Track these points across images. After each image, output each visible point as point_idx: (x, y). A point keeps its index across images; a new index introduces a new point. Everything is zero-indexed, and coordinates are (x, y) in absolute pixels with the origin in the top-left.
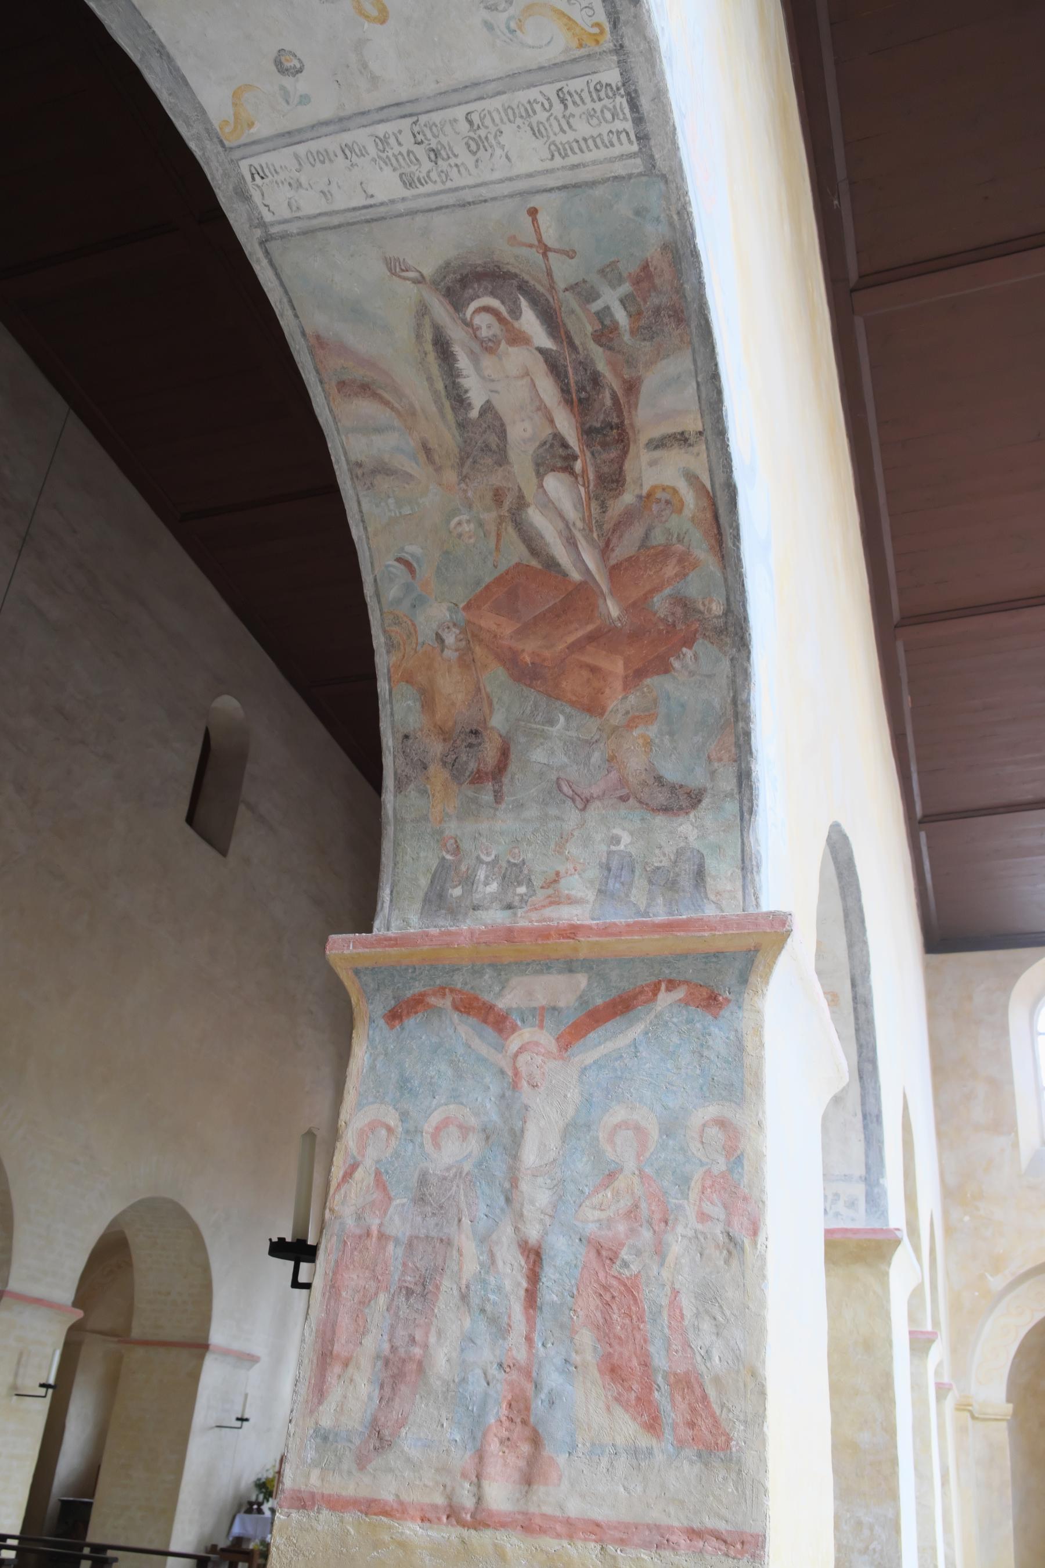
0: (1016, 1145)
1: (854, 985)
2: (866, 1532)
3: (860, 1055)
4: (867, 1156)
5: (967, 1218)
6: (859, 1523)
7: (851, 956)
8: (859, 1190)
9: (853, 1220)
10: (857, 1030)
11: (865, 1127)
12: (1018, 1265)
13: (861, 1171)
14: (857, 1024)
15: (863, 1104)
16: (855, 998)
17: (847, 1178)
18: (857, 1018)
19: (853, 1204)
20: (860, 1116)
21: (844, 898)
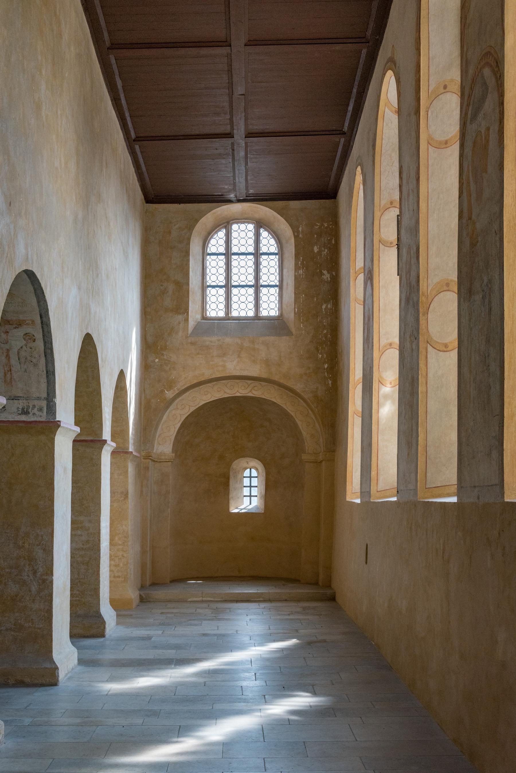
0: (187, 320)
1: (41, 317)
2: (40, 538)
3: (45, 346)
4: (48, 389)
5: (157, 360)
6: (38, 535)
7: (39, 306)
8: (44, 404)
9: (41, 416)
10: (44, 336)
11: (47, 376)
13: (45, 395)
14: (43, 333)
15: (46, 367)
16: (42, 323)
17: (39, 398)
18: (43, 331)
19: (41, 409)
20: (45, 372)
21: (33, 285)
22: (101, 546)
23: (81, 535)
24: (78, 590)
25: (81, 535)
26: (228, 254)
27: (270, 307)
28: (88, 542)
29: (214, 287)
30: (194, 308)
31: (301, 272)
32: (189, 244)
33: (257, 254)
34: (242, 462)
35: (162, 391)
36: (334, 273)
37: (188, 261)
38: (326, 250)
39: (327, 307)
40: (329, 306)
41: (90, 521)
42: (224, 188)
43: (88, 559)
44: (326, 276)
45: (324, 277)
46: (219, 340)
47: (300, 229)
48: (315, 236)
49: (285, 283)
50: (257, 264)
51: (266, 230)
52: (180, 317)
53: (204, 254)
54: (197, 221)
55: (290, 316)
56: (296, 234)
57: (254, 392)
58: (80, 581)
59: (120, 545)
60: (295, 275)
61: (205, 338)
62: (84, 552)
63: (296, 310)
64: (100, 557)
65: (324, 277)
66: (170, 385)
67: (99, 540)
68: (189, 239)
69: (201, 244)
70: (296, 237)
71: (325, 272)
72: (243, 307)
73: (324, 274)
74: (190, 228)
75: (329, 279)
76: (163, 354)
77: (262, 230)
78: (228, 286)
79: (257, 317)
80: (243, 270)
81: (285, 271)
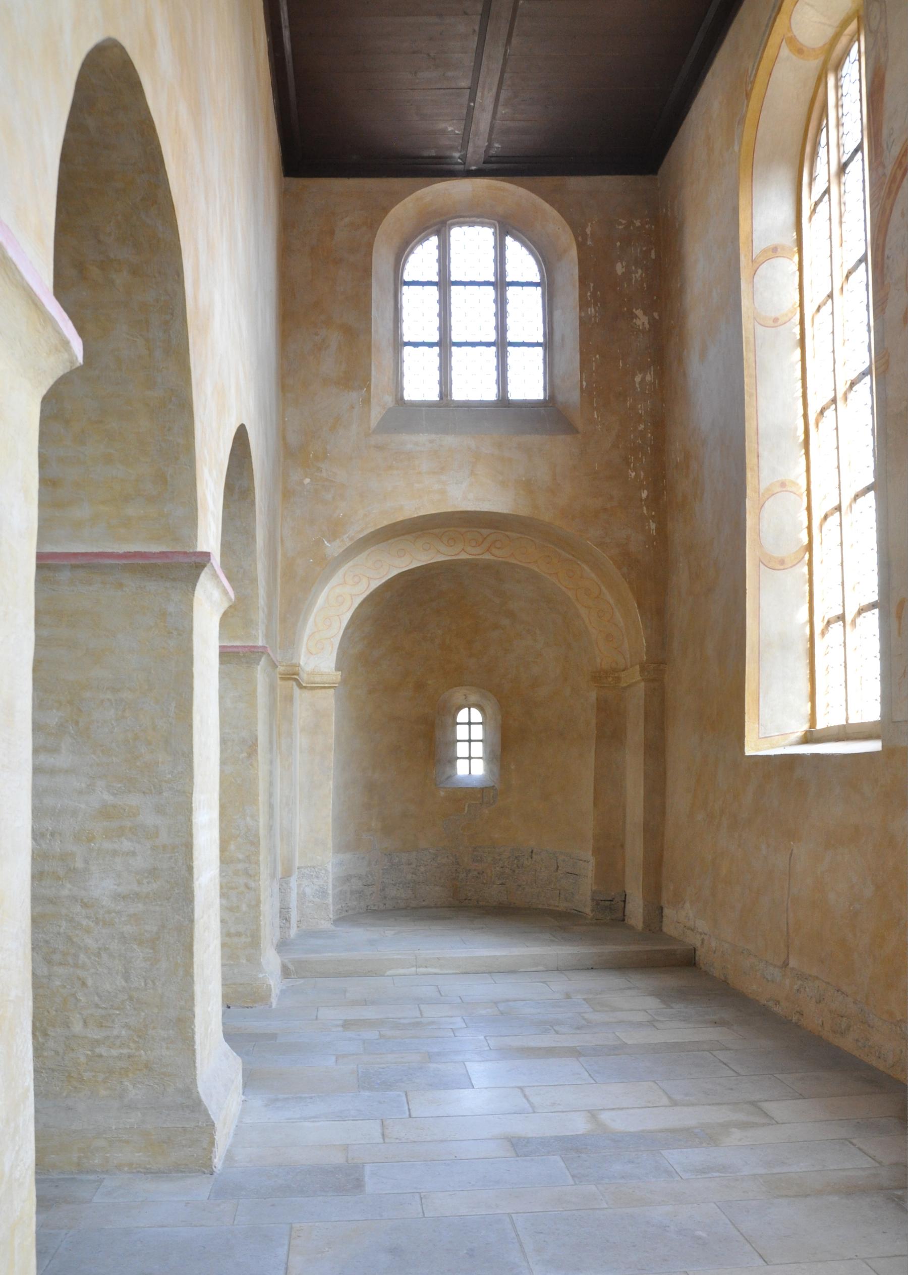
0: (367, 401)
5: (307, 481)
12: (358, 529)
22: (196, 884)
23: (134, 854)
24: (127, 1026)
25: (134, 854)
26: (444, 283)
27: (528, 382)
28: (153, 873)
29: (416, 345)
30: (379, 378)
31: (591, 311)
32: (369, 254)
33: (501, 284)
34: (458, 694)
35: (319, 543)
36: (656, 315)
37: (369, 286)
38: (640, 271)
39: (643, 379)
40: (648, 378)
41: (160, 810)
42: (444, 132)
43: (155, 929)
44: (642, 320)
45: (638, 322)
46: (431, 442)
47: (588, 230)
48: (618, 244)
49: (557, 337)
50: (501, 303)
51: (516, 238)
52: (354, 396)
53: (399, 282)
54: (386, 211)
55: (572, 396)
56: (580, 239)
57: (494, 551)
58: (131, 998)
59: (239, 861)
60: (581, 318)
61: (405, 437)
62: (141, 907)
63: (584, 383)
64: (192, 921)
65: (638, 322)
66: (335, 529)
67: (190, 869)
68: (370, 245)
69: (391, 260)
70: (581, 246)
71: (639, 312)
72: (474, 381)
73: (636, 317)
74: (373, 225)
75: (647, 326)
76: (319, 470)
77: (509, 240)
78: (445, 344)
79: (503, 402)
80: (473, 313)
81: (557, 314)
